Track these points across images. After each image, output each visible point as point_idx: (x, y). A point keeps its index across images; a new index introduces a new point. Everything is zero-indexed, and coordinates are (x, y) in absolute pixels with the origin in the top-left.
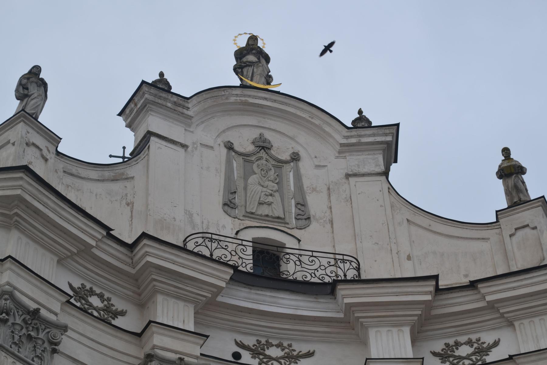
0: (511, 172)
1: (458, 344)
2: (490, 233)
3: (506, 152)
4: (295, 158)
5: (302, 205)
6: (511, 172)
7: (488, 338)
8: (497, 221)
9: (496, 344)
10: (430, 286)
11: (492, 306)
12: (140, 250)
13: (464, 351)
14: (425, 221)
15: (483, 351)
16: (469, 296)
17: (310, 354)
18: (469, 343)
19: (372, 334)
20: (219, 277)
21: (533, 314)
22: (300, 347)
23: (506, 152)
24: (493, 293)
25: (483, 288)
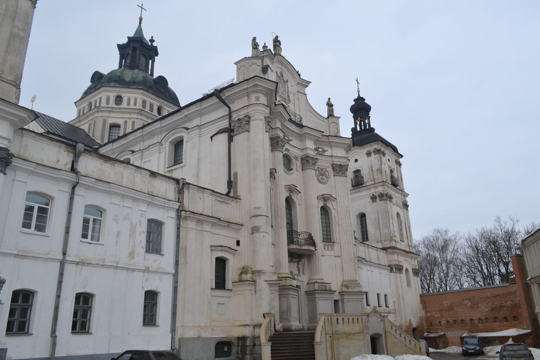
0: (330, 105)
1: (319, 148)
2: (326, 121)
3: (329, 99)
4: (287, 81)
5: (289, 96)
6: (330, 105)
7: (326, 149)
8: (328, 118)
9: (327, 151)
10: (321, 134)
11: (330, 142)
12: (278, 107)
13: (320, 150)
14: (313, 112)
15: (324, 151)
16: (326, 138)
17: (292, 140)
18: (321, 148)
19: (307, 140)
20: (287, 118)
21: (337, 147)
22: (291, 138)
23: (329, 99)
24: (332, 139)
25: (330, 137)
